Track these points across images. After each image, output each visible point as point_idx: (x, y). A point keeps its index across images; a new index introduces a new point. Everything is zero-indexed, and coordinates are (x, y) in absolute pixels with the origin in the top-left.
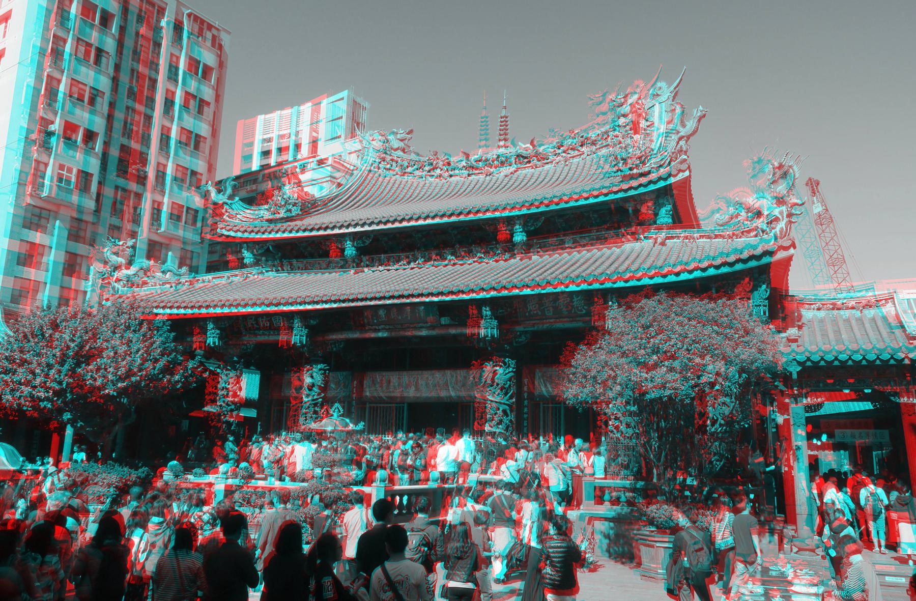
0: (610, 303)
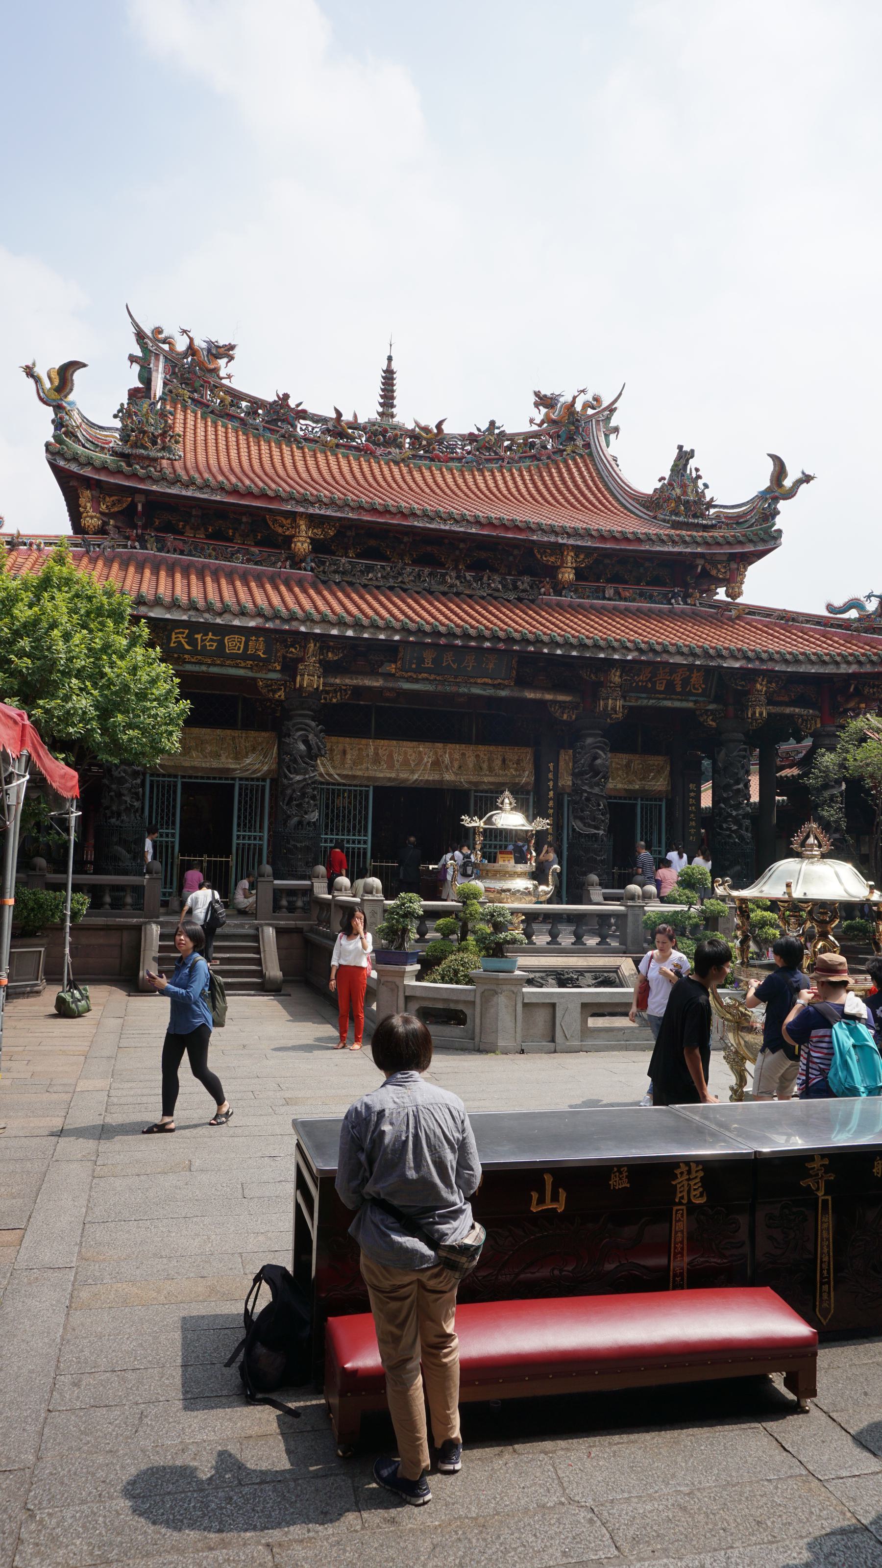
0: (759, 686)
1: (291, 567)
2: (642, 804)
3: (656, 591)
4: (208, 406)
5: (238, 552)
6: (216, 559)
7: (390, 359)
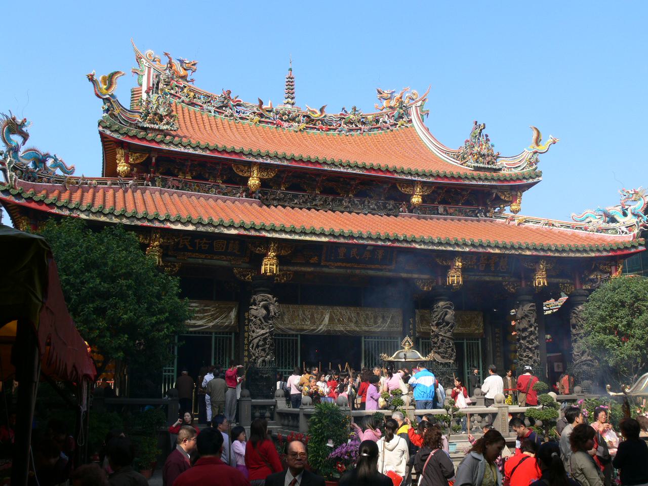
1: (246, 196)
2: (467, 343)
3: (468, 208)
4: (180, 98)
5: (212, 187)
6: (199, 192)
7: (291, 70)
